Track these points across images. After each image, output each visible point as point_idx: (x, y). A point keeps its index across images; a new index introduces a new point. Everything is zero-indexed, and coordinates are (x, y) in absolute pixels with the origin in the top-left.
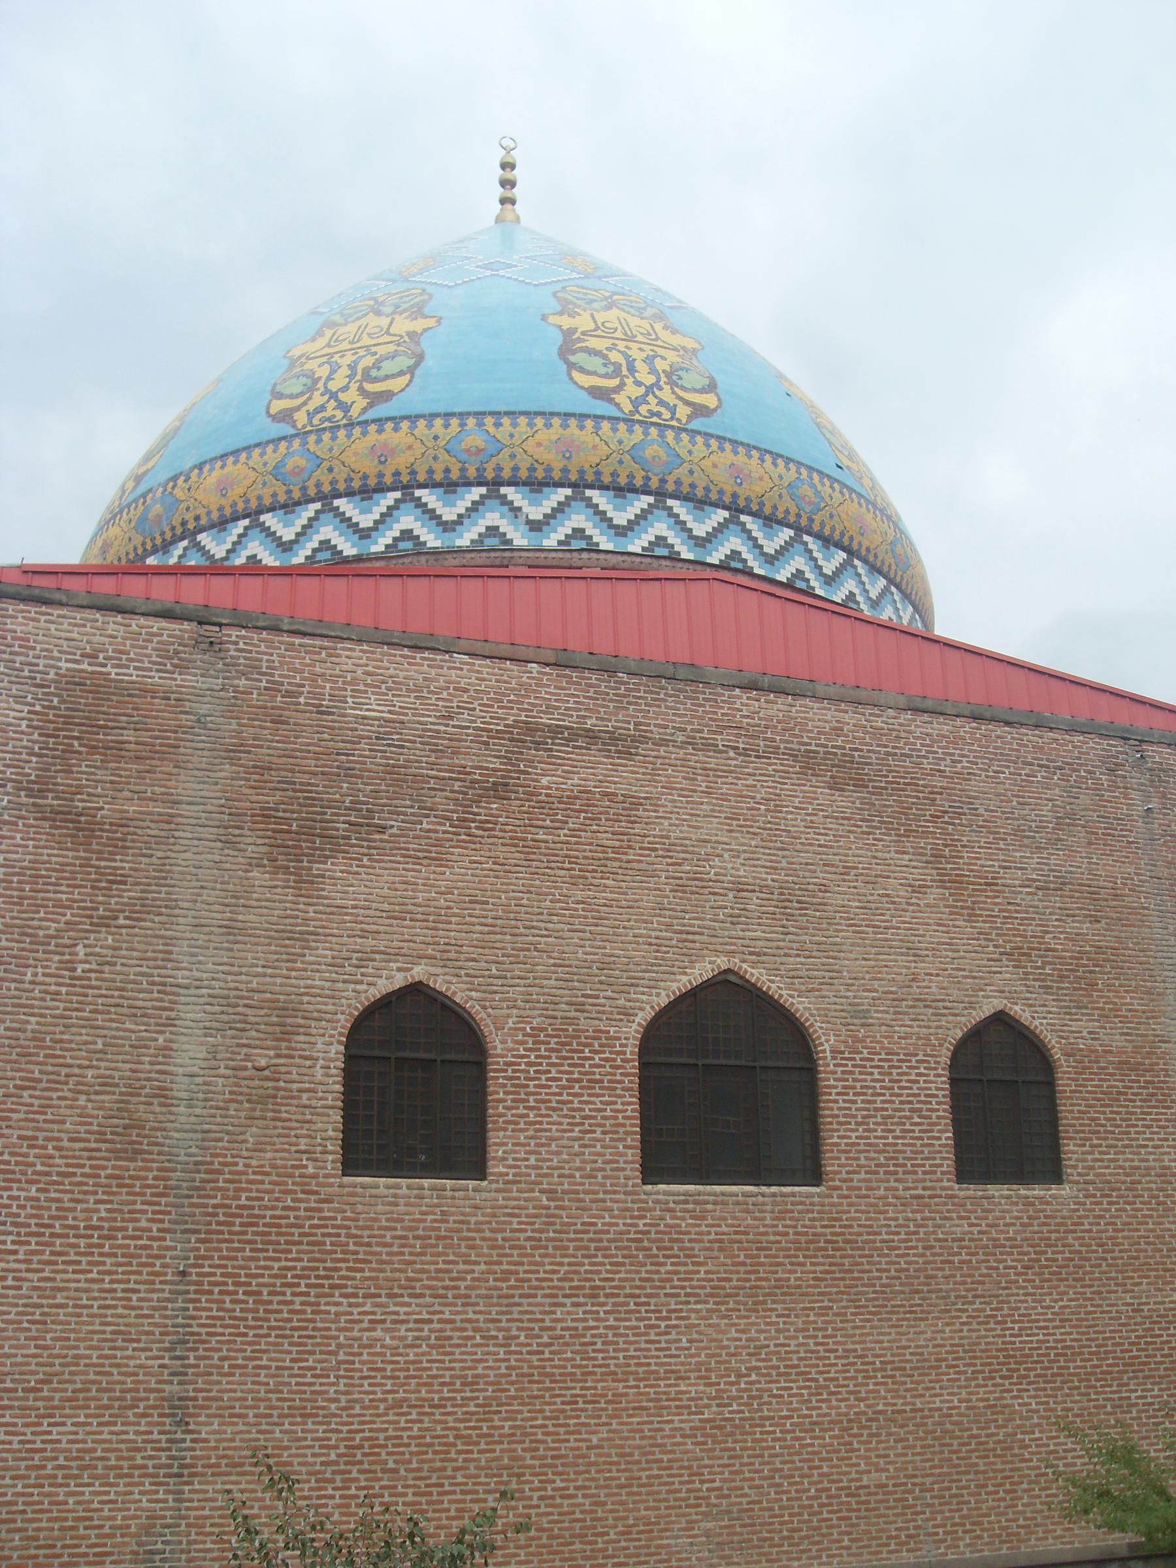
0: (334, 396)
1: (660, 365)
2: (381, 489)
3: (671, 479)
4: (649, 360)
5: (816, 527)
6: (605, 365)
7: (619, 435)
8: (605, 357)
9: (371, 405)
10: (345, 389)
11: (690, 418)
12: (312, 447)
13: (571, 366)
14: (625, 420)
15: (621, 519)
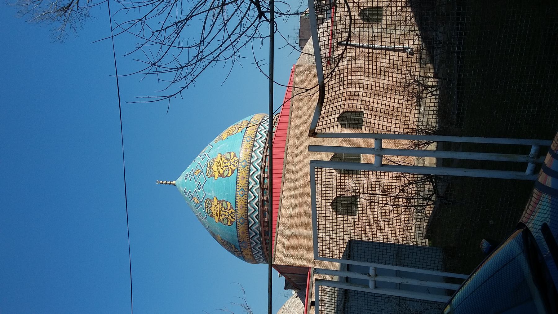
0: (229, 215)
1: (226, 161)
2: (248, 207)
3: (248, 162)
4: (225, 163)
5: (254, 138)
6: (226, 171)
7: (241, 169)
8: (225, 170)
9: (233, 209)
10: (228, 213)
11: (237, 157)
12: (239, 218)
13: (227, 176)
14: (238, 168)
15: (255, 170)
